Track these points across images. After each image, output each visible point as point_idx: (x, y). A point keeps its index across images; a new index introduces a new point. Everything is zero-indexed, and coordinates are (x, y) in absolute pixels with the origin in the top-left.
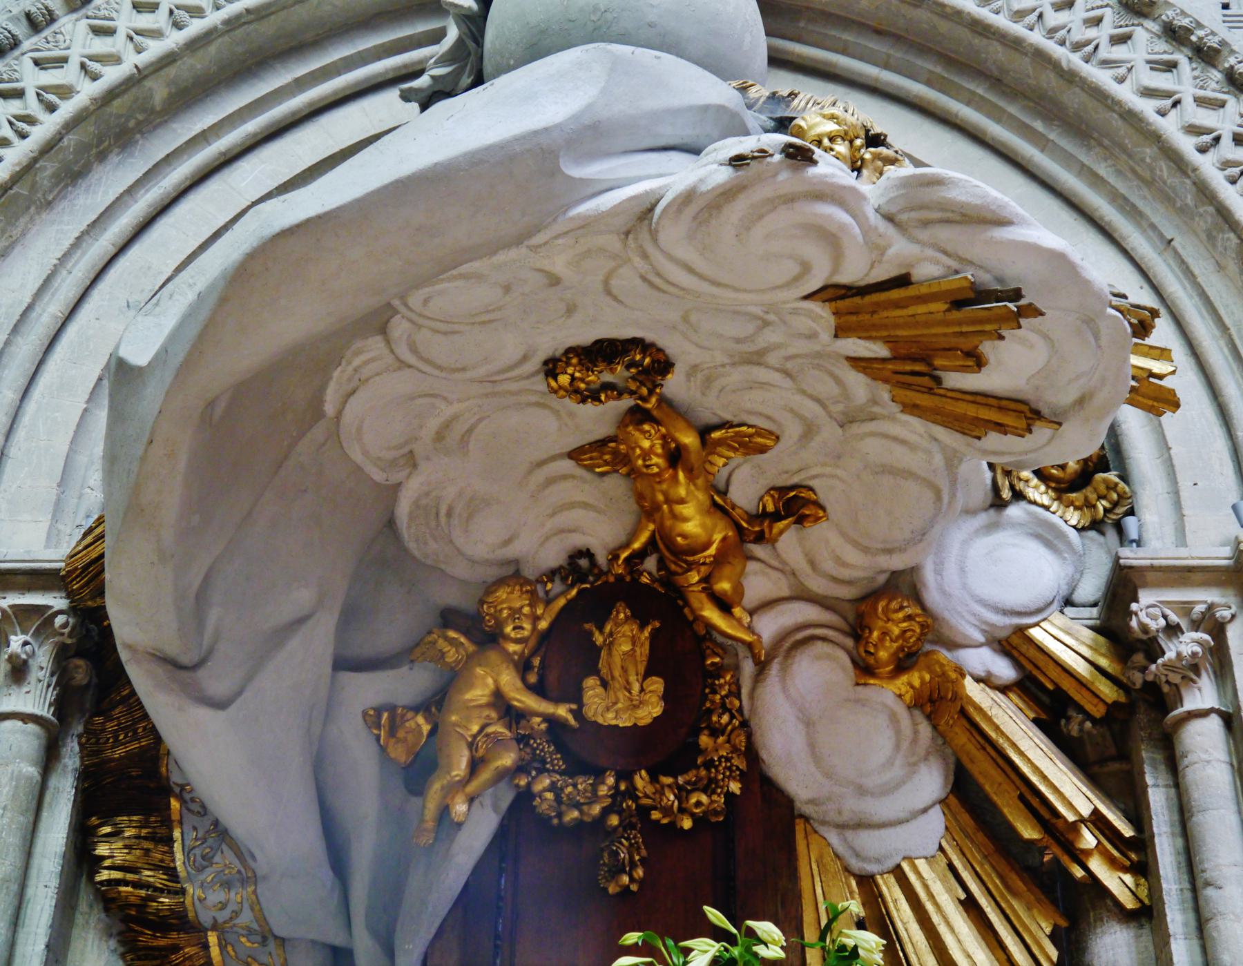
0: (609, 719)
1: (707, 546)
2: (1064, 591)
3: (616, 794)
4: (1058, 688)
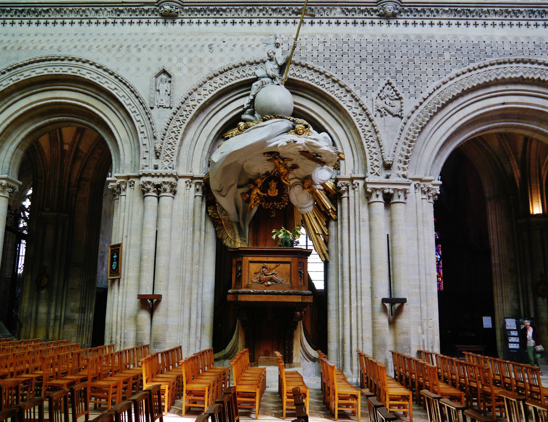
0: (271, 195)
3: (272, 205)
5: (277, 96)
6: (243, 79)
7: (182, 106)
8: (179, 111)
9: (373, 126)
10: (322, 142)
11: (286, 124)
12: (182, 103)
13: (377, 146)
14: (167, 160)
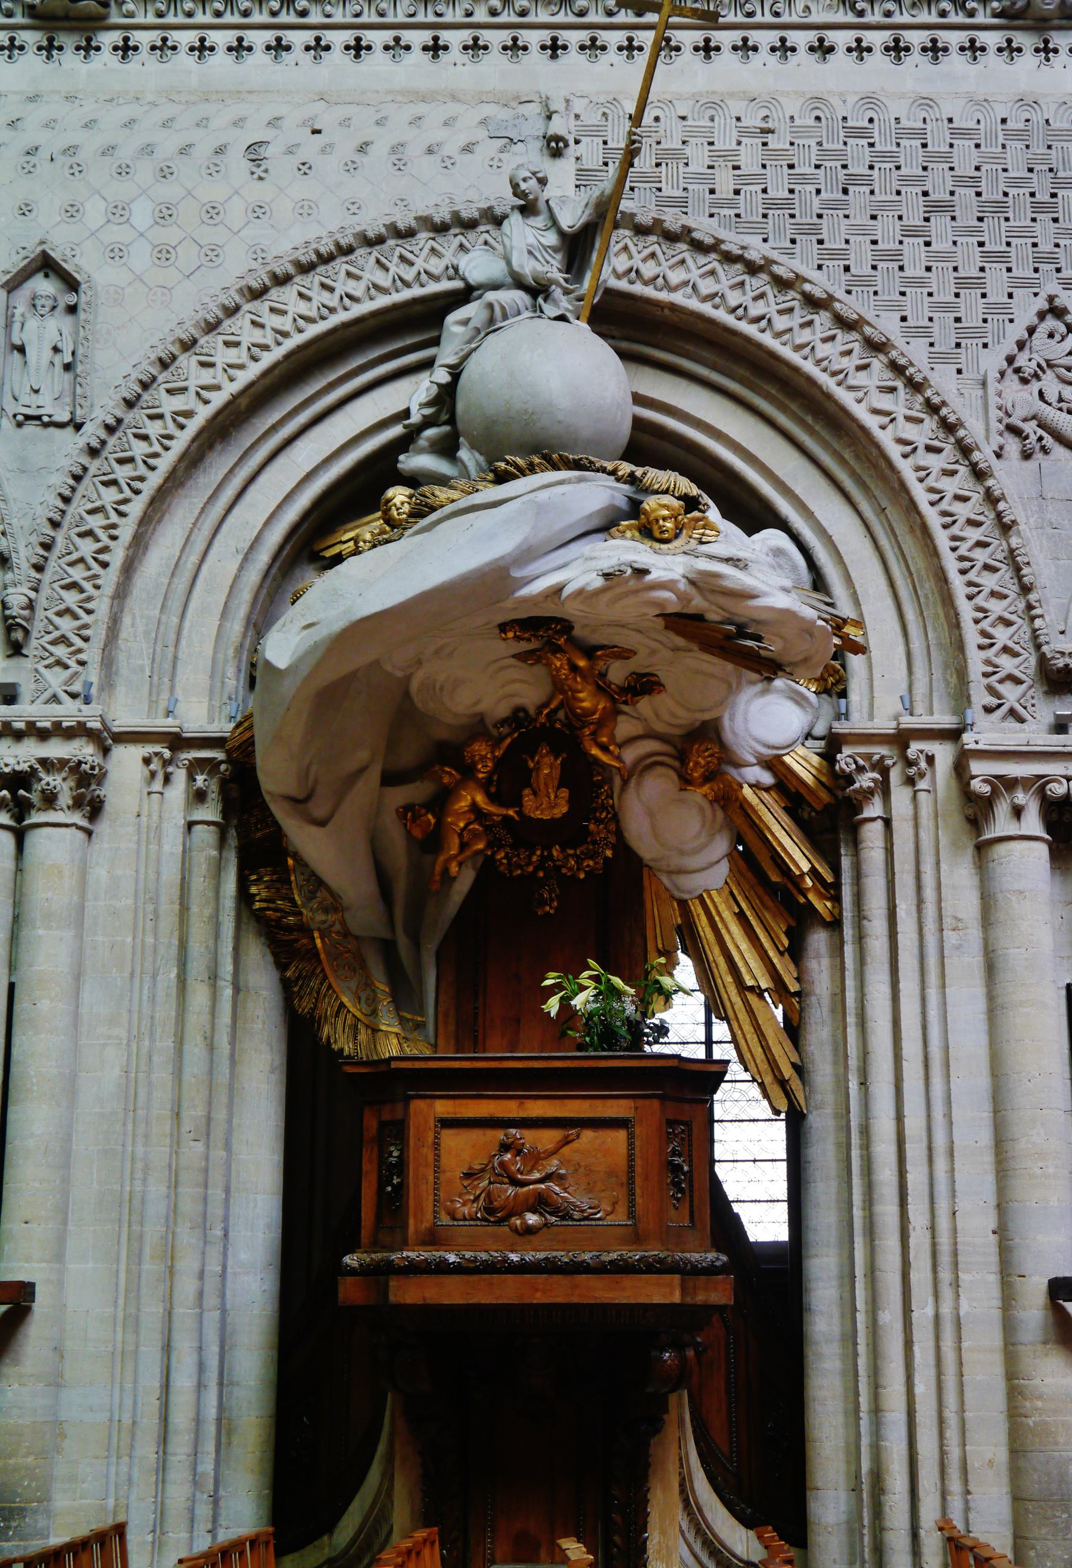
0: (538, 814)
1: (594, 714)
2: (806, 731)
4: (798, 792)
5: (556, 366)
6: (406, 294)
7: (129, 417)
8: (112, 441)
9: (991, 499)
10: (762, 572)
11: (598, 493)
12: (130, 404)
14: (59, 663)
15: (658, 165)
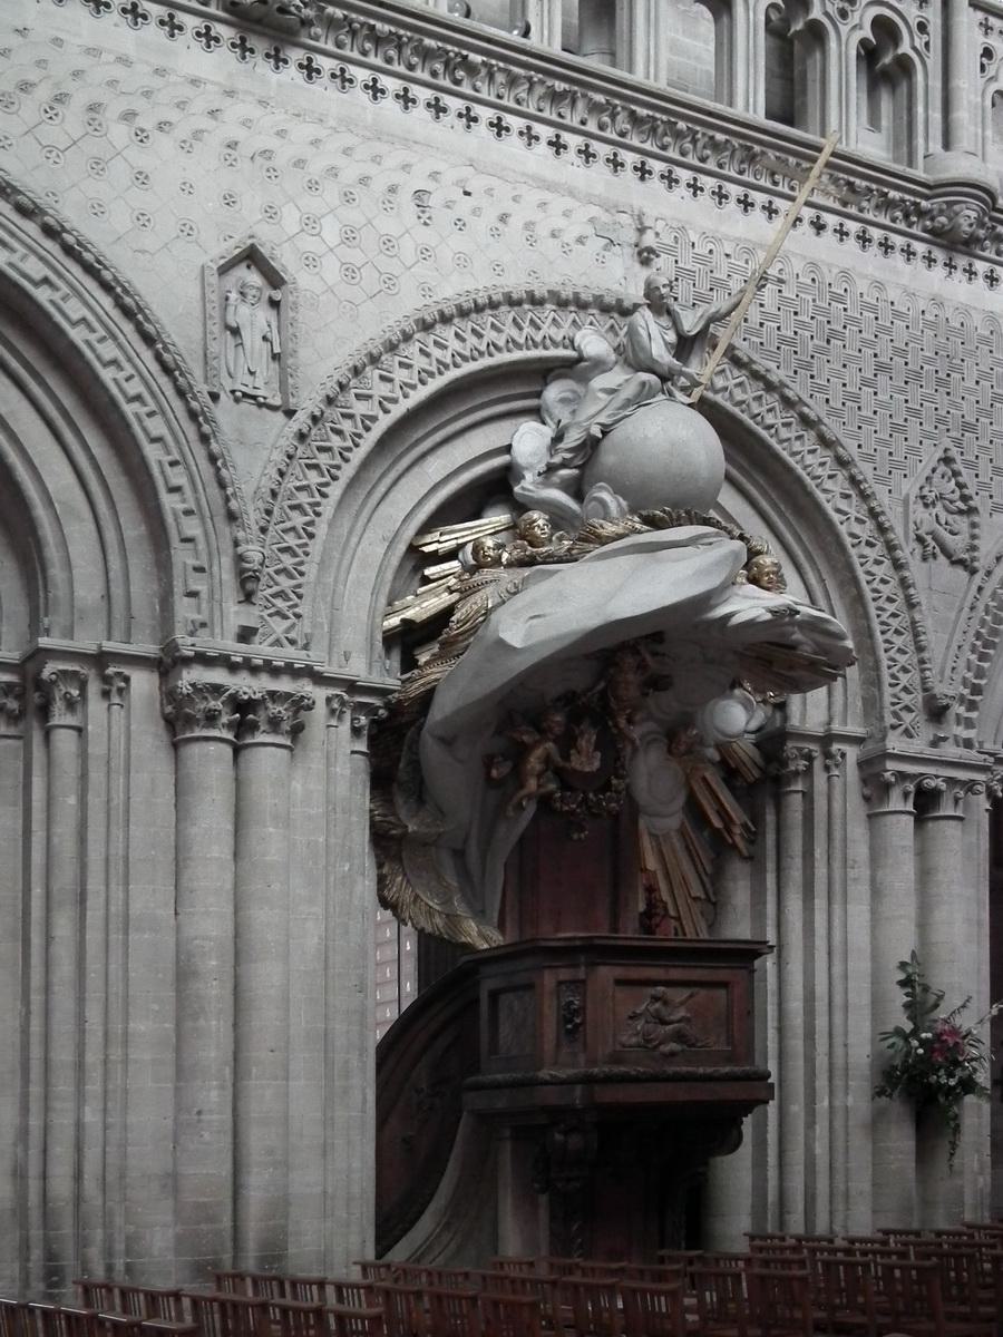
13: (911, 648)
15: (711, 289)
